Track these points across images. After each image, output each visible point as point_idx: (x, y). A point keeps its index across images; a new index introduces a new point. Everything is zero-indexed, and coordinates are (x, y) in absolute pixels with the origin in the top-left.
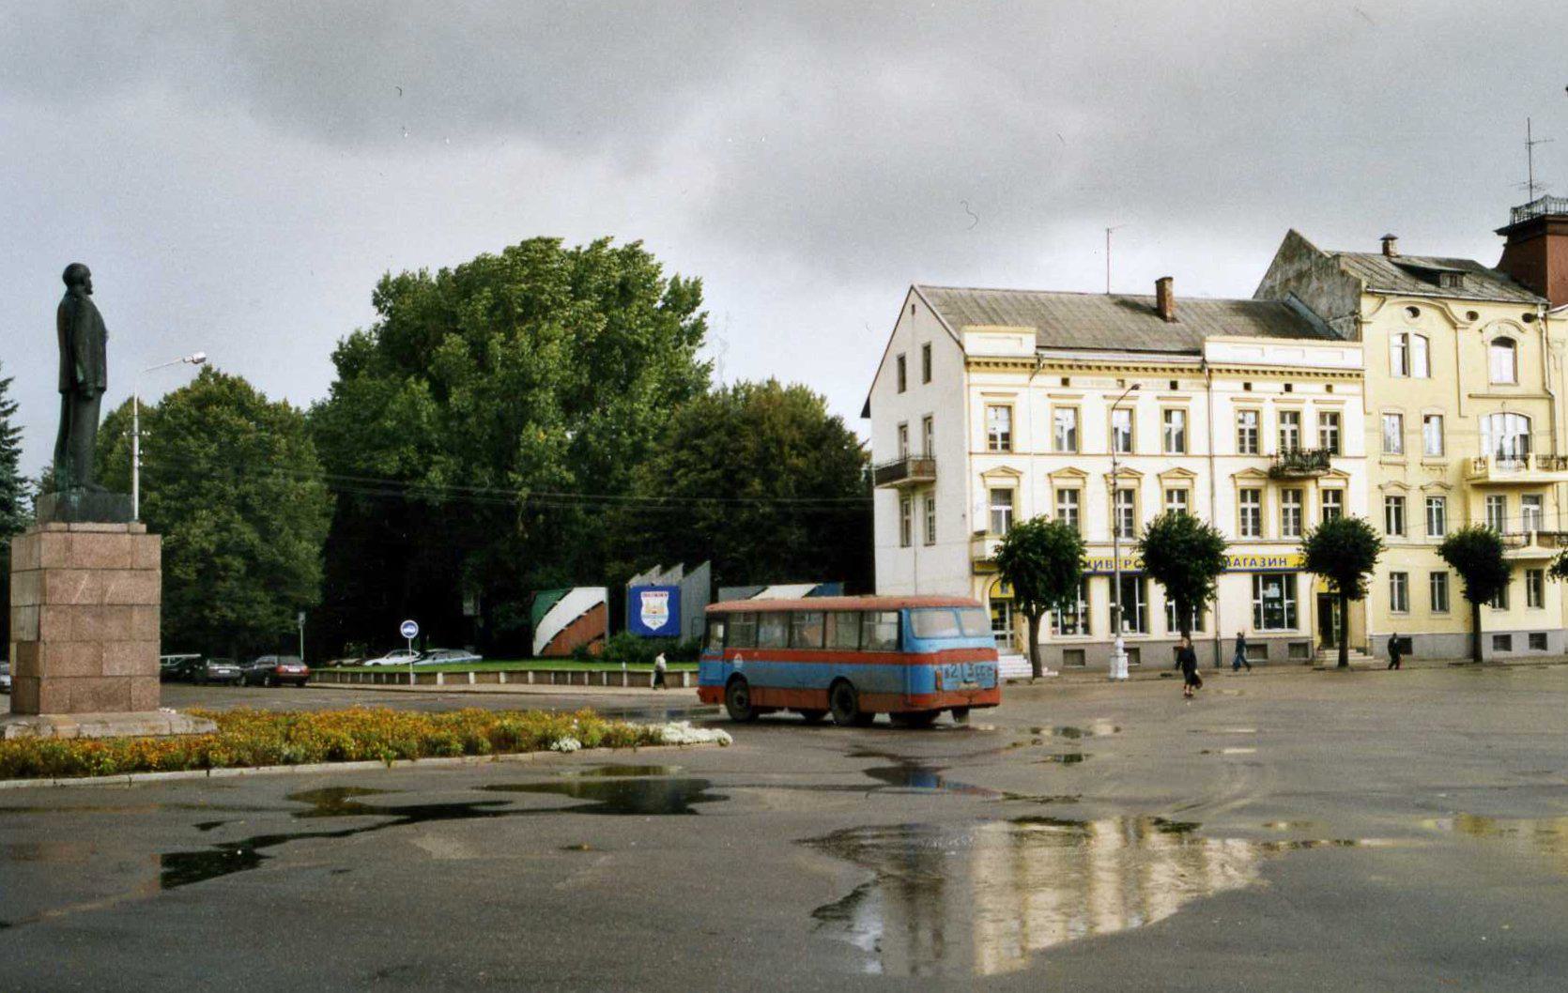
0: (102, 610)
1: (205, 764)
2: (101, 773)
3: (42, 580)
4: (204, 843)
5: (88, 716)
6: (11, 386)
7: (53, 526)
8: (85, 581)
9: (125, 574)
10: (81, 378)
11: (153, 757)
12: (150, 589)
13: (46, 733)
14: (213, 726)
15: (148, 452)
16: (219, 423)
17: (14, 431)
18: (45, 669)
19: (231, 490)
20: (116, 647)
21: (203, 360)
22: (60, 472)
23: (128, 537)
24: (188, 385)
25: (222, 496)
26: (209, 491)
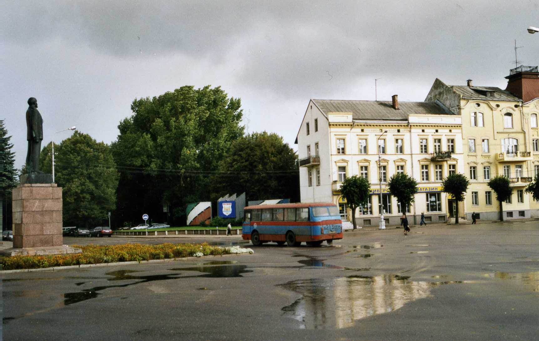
0: (43, 213)
1: (78, 263)
2: (43, 267)
3: (23, 203)
4: (78, 290)
5: (39, 248)
6: (11, 138)
7: (26, 185)
8: (37, 203)
9: (50, 200)
10: (34, 135)
11: (61, 261)
12: (59, 205)
13: (25, 254)
14: (81, 251)
15: (57, 160)
16: (81, 150)
17: (12, 154)
18: (24, 233)
19: (85, 172)
20: (48, 225)
21: (75, 129)
22: (28, 167)
23: (51, 188)
24: (70, 137)
25: (82, 174)
26: (78, 172)
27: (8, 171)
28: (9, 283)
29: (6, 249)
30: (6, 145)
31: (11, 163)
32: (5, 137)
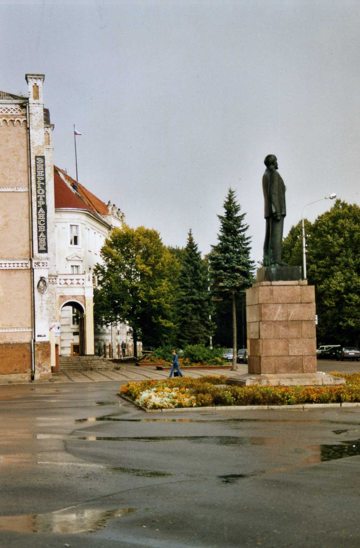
0: (288, 323)
1: (339, 400)
2: (289, 403)
3: (260, 309)
4: (336, 440)
5: (283, 375)
6: (245, 217)
7: (264, 283)
8: (280, 309)
9: (298, 305)
10: (274, 210)
11: (314, 396)
12: (310, 314)
13: (264, 383)
14: (343, 381)
15: (311, 245)
16: (343, 227)
17: (248, 238)
18: (263, 352)
19: (351, 261)
20: (295, 341)
21: (335, 197)
22: (266, 256)
23: (299, 287)
24: (217, 242)
25: (347, 265)
26: (340, 263)
27: (243, 264)
28: (240, 424)
29: (240, 376)
30: (239, 226)
31: (246, 252)
32: (237, 215)
